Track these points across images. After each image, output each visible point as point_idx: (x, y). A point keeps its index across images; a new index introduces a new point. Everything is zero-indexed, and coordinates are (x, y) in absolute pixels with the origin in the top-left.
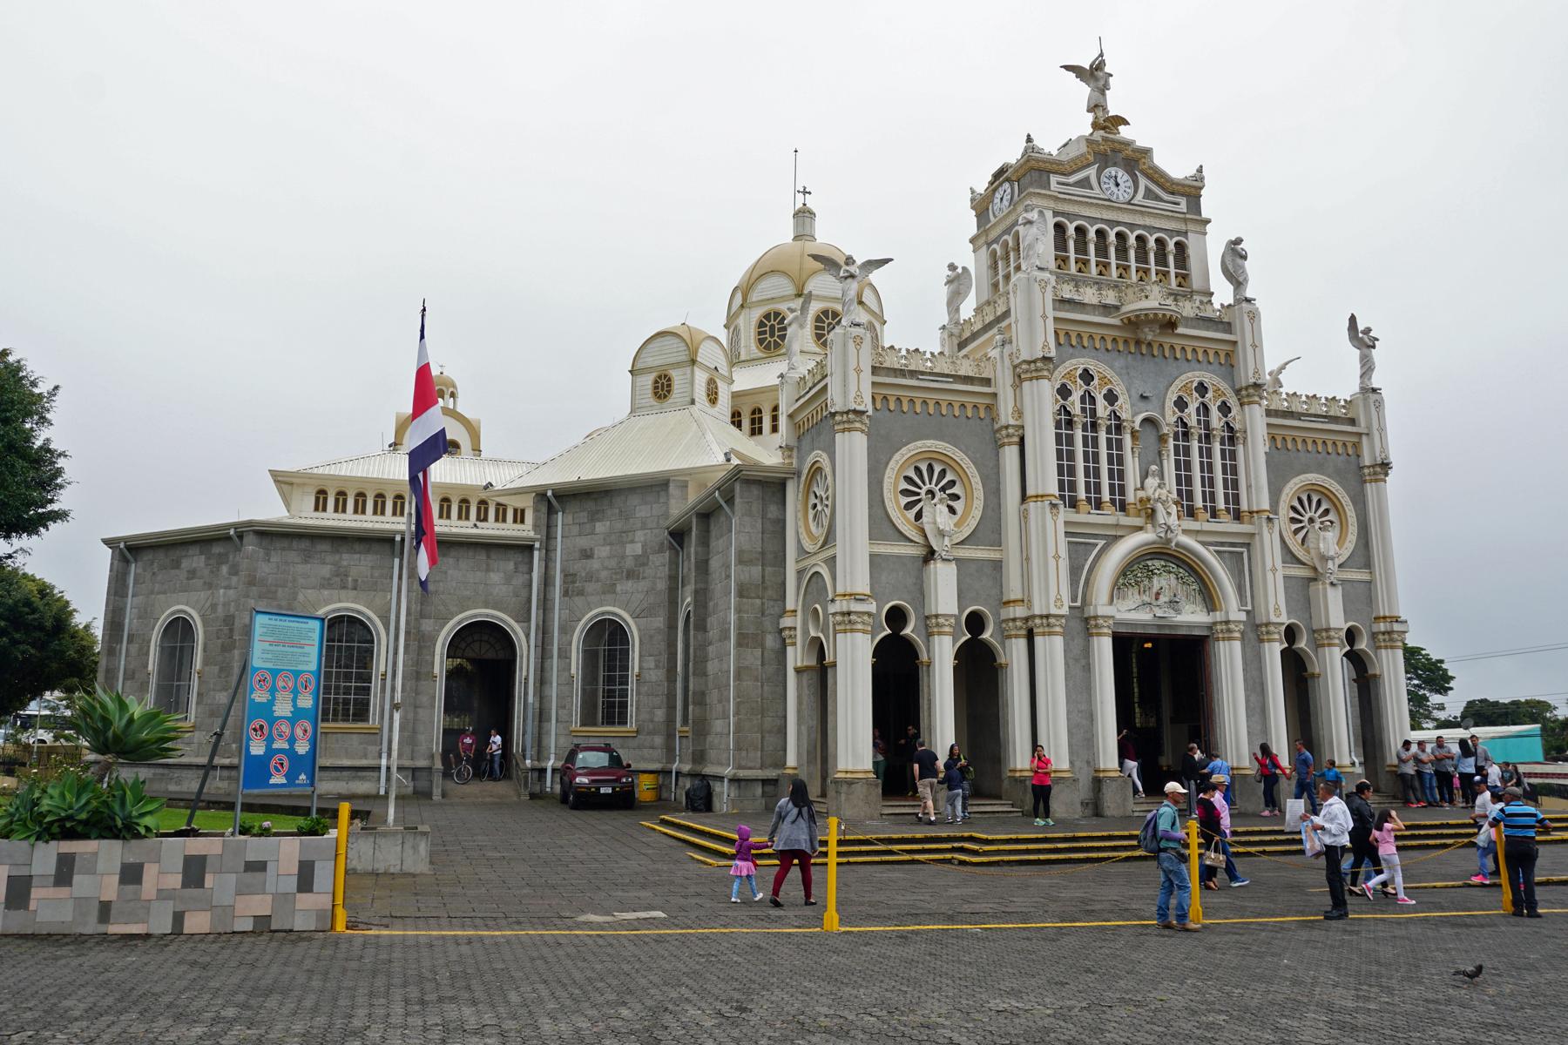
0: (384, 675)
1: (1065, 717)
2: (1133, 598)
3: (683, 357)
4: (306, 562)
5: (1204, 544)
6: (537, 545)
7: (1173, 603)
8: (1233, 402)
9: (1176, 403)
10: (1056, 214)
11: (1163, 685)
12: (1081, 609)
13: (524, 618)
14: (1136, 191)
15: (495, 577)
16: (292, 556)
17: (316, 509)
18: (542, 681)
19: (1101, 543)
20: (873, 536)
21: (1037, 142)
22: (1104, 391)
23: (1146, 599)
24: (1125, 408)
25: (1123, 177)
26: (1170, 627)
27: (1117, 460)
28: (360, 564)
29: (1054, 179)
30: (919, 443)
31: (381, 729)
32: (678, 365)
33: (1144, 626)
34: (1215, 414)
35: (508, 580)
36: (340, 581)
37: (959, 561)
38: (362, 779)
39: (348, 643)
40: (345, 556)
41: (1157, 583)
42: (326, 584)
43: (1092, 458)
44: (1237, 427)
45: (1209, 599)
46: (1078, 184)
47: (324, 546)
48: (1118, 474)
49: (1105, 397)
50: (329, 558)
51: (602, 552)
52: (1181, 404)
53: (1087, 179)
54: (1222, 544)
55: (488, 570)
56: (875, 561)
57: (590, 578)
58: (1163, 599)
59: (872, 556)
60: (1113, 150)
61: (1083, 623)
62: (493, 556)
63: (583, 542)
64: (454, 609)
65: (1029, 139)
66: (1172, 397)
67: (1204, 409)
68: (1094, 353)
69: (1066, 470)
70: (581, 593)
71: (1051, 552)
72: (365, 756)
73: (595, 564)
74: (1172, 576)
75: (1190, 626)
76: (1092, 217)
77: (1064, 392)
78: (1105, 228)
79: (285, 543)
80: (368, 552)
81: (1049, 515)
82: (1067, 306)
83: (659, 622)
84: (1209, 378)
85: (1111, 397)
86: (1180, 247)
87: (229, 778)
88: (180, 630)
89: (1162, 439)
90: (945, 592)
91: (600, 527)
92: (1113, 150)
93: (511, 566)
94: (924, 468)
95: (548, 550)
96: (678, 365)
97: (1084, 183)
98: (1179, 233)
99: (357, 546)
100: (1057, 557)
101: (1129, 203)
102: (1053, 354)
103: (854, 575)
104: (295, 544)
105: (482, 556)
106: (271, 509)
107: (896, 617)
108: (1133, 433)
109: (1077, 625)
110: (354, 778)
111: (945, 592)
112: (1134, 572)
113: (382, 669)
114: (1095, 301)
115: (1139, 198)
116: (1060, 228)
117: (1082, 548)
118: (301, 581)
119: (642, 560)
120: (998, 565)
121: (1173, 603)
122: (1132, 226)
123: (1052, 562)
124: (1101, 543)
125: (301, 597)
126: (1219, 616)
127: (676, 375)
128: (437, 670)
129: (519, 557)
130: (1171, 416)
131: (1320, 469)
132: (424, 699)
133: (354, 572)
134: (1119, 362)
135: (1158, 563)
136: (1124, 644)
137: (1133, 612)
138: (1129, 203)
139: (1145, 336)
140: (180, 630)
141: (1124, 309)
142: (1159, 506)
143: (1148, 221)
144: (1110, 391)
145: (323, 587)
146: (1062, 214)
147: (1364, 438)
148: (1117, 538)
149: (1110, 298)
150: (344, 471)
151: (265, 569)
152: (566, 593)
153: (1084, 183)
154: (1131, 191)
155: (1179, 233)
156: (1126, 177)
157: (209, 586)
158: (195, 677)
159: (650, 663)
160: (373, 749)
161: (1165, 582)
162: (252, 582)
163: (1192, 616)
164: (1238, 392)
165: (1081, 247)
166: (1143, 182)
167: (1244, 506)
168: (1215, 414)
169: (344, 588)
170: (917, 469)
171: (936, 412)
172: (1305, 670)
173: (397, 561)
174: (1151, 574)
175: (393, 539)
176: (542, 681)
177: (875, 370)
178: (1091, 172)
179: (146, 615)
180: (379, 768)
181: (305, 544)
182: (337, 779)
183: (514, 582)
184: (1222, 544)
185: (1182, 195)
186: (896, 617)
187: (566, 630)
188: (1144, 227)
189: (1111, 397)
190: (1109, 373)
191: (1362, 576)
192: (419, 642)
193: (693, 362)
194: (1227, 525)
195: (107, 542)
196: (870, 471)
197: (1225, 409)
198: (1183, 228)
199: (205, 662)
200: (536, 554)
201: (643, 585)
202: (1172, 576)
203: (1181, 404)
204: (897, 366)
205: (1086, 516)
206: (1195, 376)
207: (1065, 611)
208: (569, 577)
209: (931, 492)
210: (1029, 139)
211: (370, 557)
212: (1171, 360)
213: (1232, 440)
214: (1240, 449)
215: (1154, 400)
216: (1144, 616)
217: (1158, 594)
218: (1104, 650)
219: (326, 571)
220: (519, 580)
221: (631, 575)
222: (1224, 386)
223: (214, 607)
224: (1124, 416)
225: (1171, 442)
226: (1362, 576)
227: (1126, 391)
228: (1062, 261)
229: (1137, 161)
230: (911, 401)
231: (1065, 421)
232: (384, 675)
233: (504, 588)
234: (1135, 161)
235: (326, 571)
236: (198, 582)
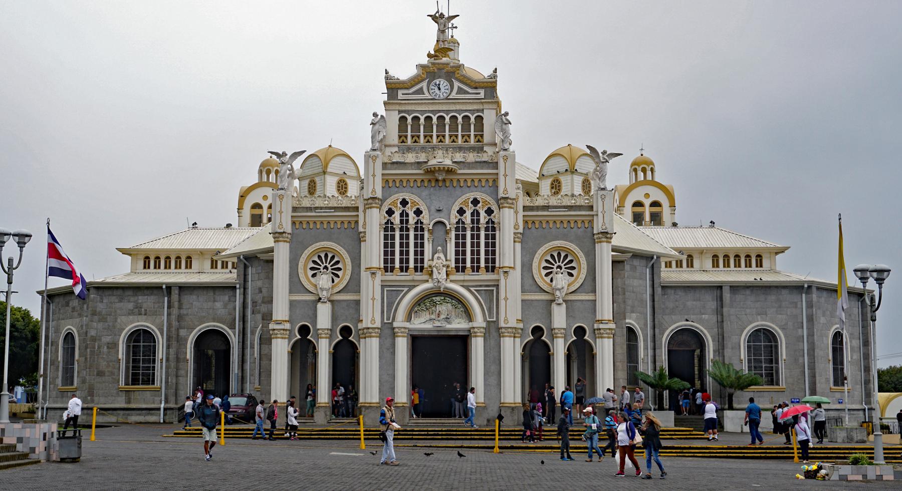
0: (162, 360)
1: (385, 378)
2: (425, 316)
3: (321, 170)
4: (120, 301)
5: (467, 288)
6: (238, 286)
7: (447, 319)
8: (494, 207)
9: (458, 212)
10: (400, 112)
11: (440, 364)
12: (391, 323)
13: (232, 327)
14: (451, 91)
15: (218, 305)
16: (114, 299)
17: (145, 268)
18: (243, 361)
19: (406, 289)
20: (291, 292)
21: (391, 73)
22: (414, 209)
23: (433, 317)
24: (425, 218)
25: (443, 83)
26: (445, 331)
28: (148, 301)
29: (400, 92)
30: (318, 244)
31: (161, 388)
32: (318, 174)
33: (429, 331)
34: (483, 214)
35: (225, 306)
36: (138, 311)
37: (332, 301)
38: (152, 414)
39: (141, 342)
40: (140, 297)
41: (439, 308)
42: (131, 313)
43: (404, 245)
44: (496, 221)
45: (469, 316)
46: (413, 93)
47: (130, 293)
49: (415, 212)
50: (132, 299)
52: (461, 212)
53: (421, 89)
54: (481, 286)
55: (214, 301)
56: (292, 304)
58: (442, 317)
59: (358, 291)
60: (439, 69)
61: (388, 332)
62: (217, 292)
64: (197, 323)
65: (387, 72)
66: (456, 208)
68: (410, 189)
69: (388, 253)
71: (371, 296)
72: (154, 403)
74: (449, 305)
75: (457, 330)
76: (421, 110)
77: (390, 212)
78: (442, 109)
79: (110, 292)
80: (151, 294)
81: (370, 278)
82: (395, 166)
84: (479, 196)
85: (418, 212)
86: (480, 119)
87: (87, 414)
88: (69, 337)
89: (447, 232)
90: (324, 318)
92: (439, 69)
93: (227, 298)
94: (323, 256)
95: (245, 289)
96: (318, 174)
97: (420, 91)
98: (478, 111)
99: (145, 291)
100: (373, 299)
101: (447, 99)
102: (379, 194)
103: (281, 310)
104: (115, 292)
105: (211, 293)
106: (121, 271)
107: (304, 330)
108: (431, 232)
109: (387, 332)
110: (148, 414)
111: (324, 318)
112: (425, 301)
113: (160, 357)
114: (413, 161)
115: (454, 95)
116: (403, 119)
117: (391, 294)
118: (118, 311)
121: (447, 319)
122: (447, 112)
123: (371, 302)
124: (406, 289)
125: (119, 320)
126: (471, 325)
127: (317, 179)
128: (188, 357)
129: (231, 293)
130: (454, 217)
131: (565, 238)
132: (182, 372)
133: (145, 306)
134: (425, 193)
135: (438, 298)
136: (417, 341)
137: (423, 323)
138: (447, 99)
139: (437, 179)
140: (69, 337)
141: (430, 163)
142: (435, 269)
143: (458, 107)
144: (418, 209)
145: (129, 314)
146: (404, 111)
147: (595, 217)
148: (415, 286)
149: (422, 157)
150: (158, 245)
151: (101, 307)
152: (253, 313)
153: (420, 91)
154: (448, 92)
155: (478, 111)
156: (446, 83)
157: (80, 315)
158: (76, 363)
160: (157, 399)
161: (445, 308)
162: (94, 313)
163: (458, 325)
164: (497, 201)
165: (415, 128)
166: (456, 84)
167: (497, 265)
168: (483, 214)
169: (140, 314)
170: (319, 257)
171: (324, 230)
172: (549, 350)
173: (166, 299)
174: (435, 304)
175: (161, 287)
176: (243, 361)
177: (295, 209)
178: (424, 84)
179: (57, 331)
180: (159, 409)
181: (119, 292)
182: (140, 415)
183: (228, 307)
184: (481, 286)
185: (482, 88)
186: (304, 330)
187: (253, 333)
188: (456, 111)
189: (418, 212)
190: (417, 199)
191: (590, 297)
192: (175, 340)
193: (324, 173)
194: (483, 276)
195: (38, 292)
196: (290, 262)
197: (489, 212)
198: (480, 107)
199: (80, 356)
200: (238, 291)
202: (449, 305)
203: (461, 212)
204: (309, 206)
205: (396, 277)
206: (471, 196)
207: (378, 324)
208: (254, 303)
209: (326, 268)
210: (387, 72)
211: (152, 297)
212: (458, 188)
213: (494, 229)
214: (497, 233)
215: (445, 211)
216: (429, 326)
217: (439, 315)
218: (402, 346)
219: (131, 306)
220: (230, 306)
222: (488, 199)
223: (82, 326)
224: (425, 221)
225: (453, 233)
226: (590, 297)
227: (427, 207)
228: (402, 138)
229: (454, 73)
230: (322, 223)
231: (388, 227)
232: (162, 360)
233: (223, 311)
234: (454, 73)
235: (131, 306)
236: (76, 314)
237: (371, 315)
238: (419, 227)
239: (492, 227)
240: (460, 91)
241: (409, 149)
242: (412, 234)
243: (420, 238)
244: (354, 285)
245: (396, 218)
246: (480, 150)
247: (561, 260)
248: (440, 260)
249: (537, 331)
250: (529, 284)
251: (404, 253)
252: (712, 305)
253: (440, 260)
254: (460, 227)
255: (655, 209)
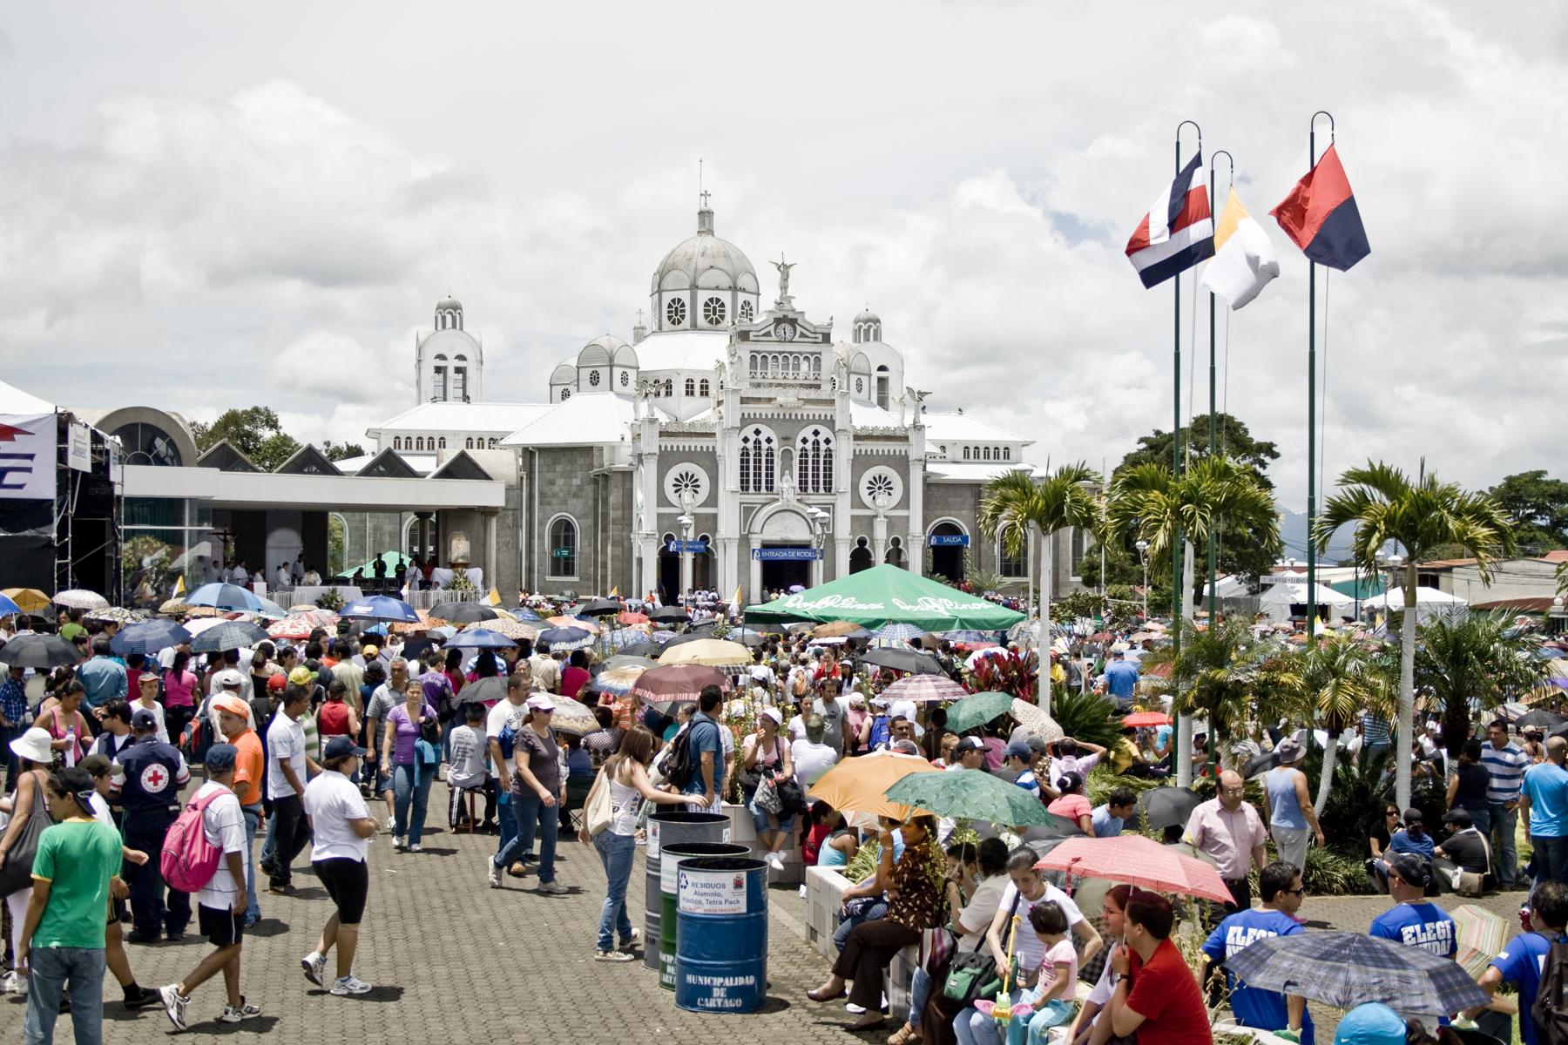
8: (832, 438)
24: (774, 445)
25: (788, 328)
27: (770, 468)
48: (770, 475)
51: (560, 482)
52: (805, 441)
57: (555, 495)
63: (549, 476)
67: (816, 443)
70: (549, 504)
73: (556, 489)
77: (746, 440)
83: (590, 521)
91: (559, 468)
97: (768, 334)
115: (796, 338)
116: (753, 358)
117: (748, 512)
119: (580, 488)
120: (715, 516)
137: (774, 533)
153: (768, 334)
159: (586, 543)
166: (799, 329)
187: (542, 524)
189: (769, 440)
201: (581, 501)
208: (542, 495)
221: (575, 496)
237: (728, 526)
238: (770, 453)
239: (829, 453)
240: (802, 335)
241: (759, 385)
242: (764, 459)
243: (770, 462)
244: (712, 500)
245: (750, 445)
246: (818, 387)
247: (881, 484)
248: (787, 484)
249: (862, 542)
250: (857, 502)
251: (757, 475)
252: (970, 501)
253: (787, 484)
254: (804, 453)
255: (883, 374)
